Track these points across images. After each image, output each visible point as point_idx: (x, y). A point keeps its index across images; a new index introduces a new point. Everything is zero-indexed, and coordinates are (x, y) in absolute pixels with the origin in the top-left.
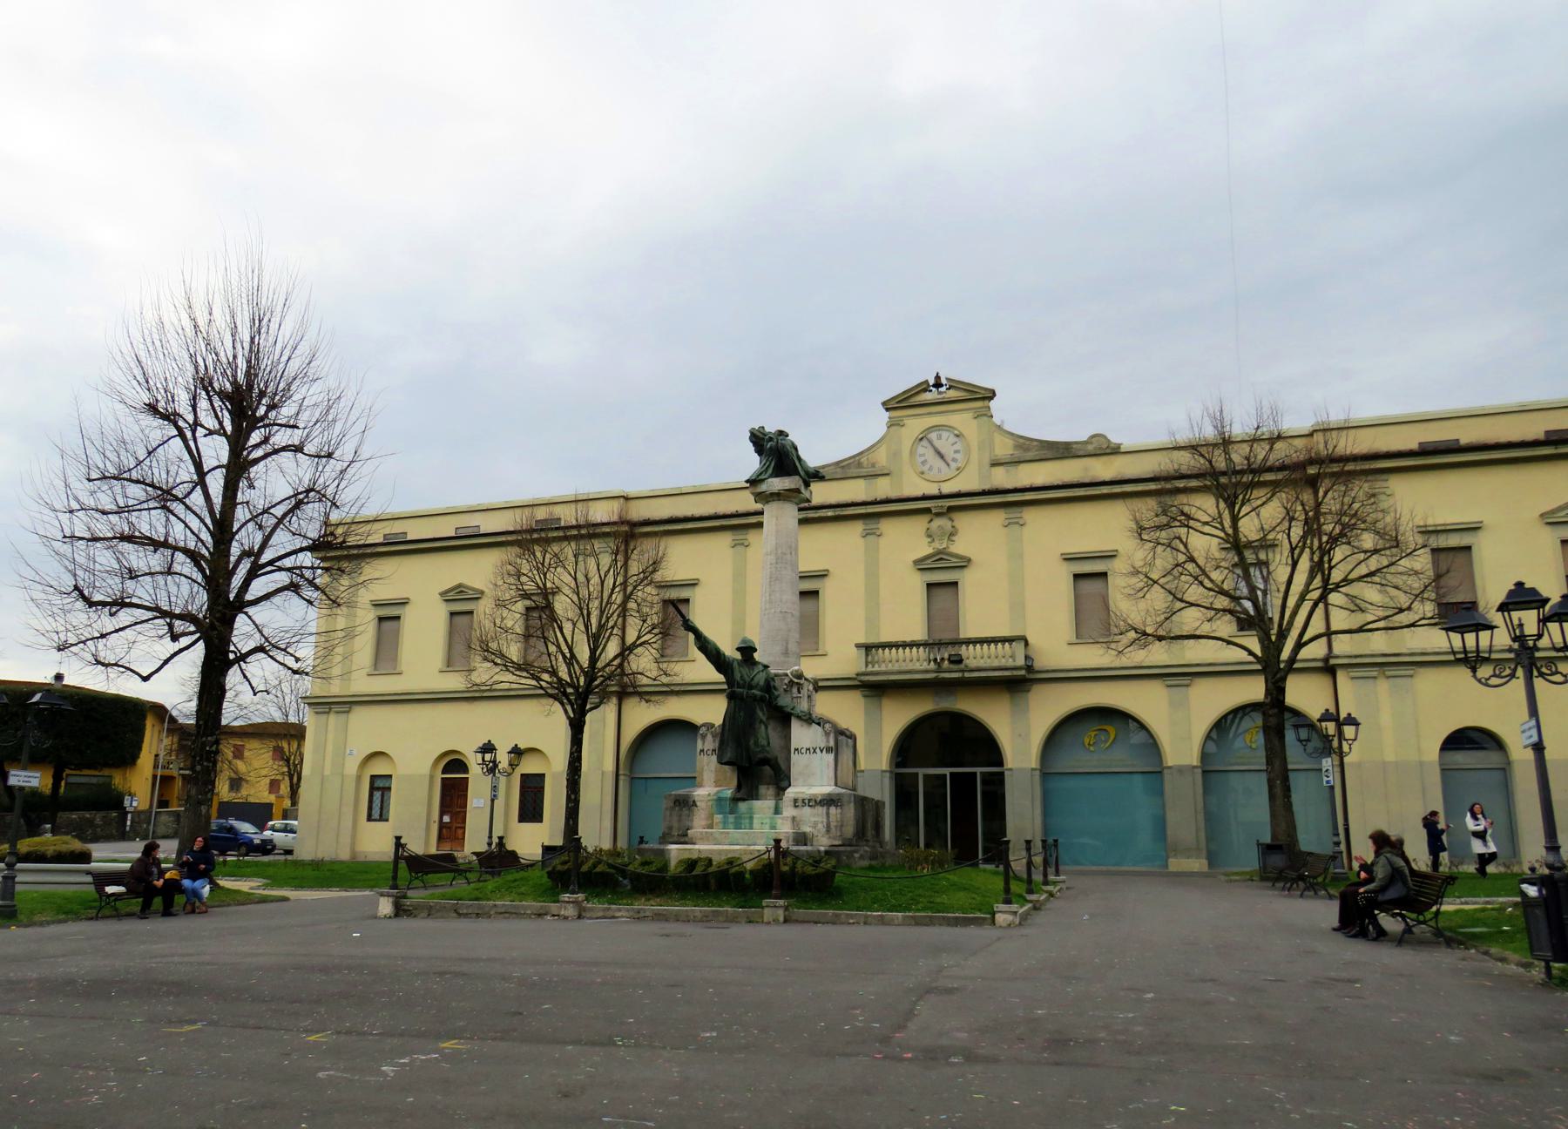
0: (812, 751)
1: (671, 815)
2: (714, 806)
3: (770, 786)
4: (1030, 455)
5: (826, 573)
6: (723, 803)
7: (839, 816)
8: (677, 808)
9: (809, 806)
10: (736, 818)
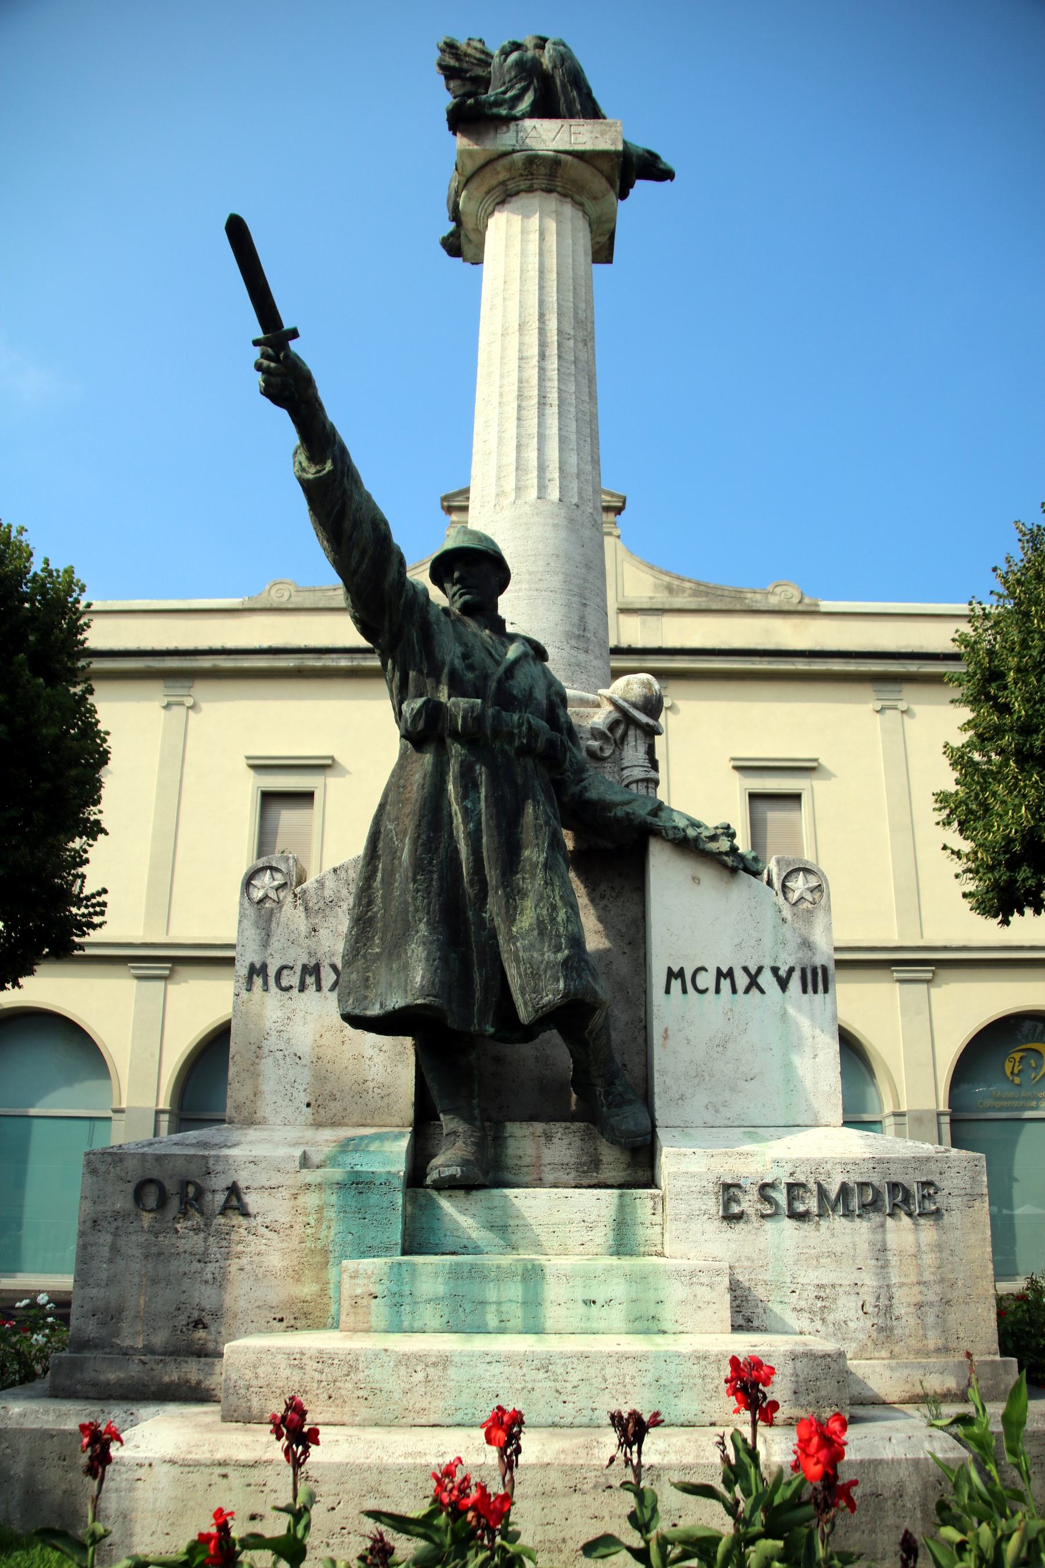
0: (742, 980)
1: (115, 1250)
2: (331, 1213)
3: (557, 1128)
4: (679, 602)
5: (329, 762)
6: (374, 1198)
7: (929, 1259)
8: (147, 1219)
9: (794, 1215)
10: (455, 1274)
